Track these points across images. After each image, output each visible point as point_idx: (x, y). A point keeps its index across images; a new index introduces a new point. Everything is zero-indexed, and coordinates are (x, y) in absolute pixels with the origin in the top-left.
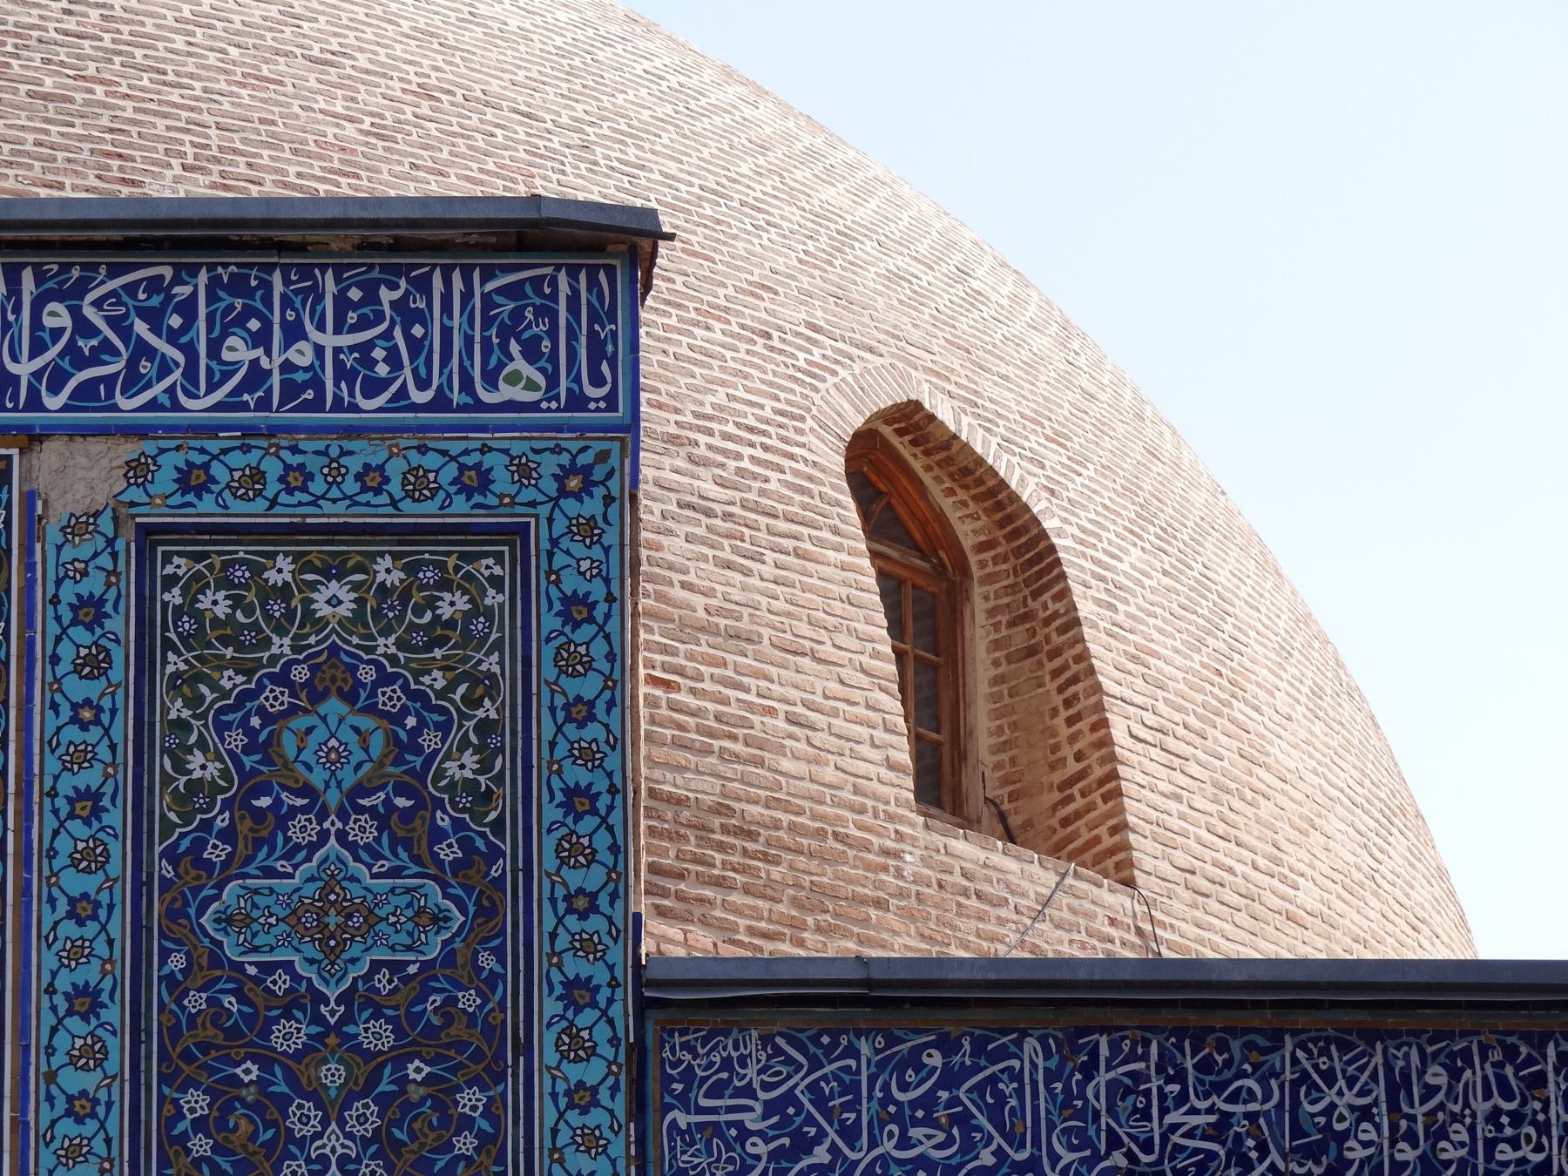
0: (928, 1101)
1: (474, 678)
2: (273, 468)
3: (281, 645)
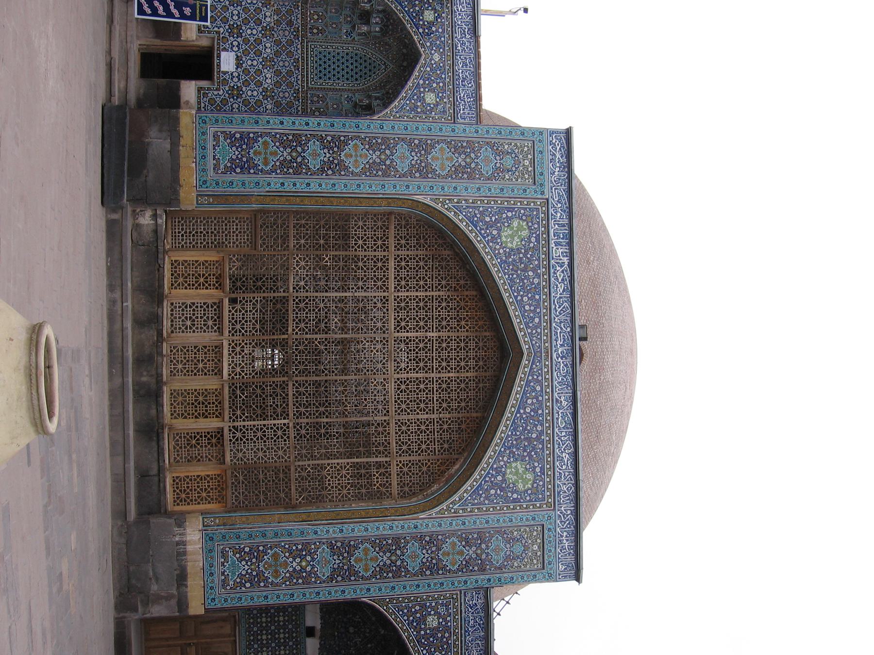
0: (477, 622)
1: (526, 565)
2: (551, 539)
3: (530, 542)
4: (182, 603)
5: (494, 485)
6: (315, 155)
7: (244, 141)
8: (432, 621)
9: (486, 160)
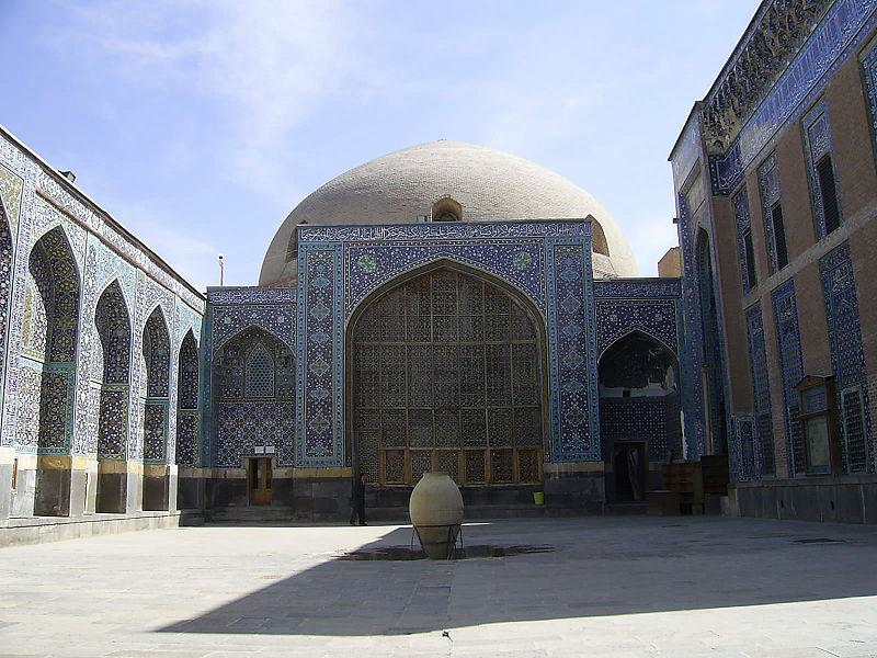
4: (597, 474)
5: (528, 278)
6: (319, 393)
7: (311, 437)
8: (613, 318)
9: (321, 282)
